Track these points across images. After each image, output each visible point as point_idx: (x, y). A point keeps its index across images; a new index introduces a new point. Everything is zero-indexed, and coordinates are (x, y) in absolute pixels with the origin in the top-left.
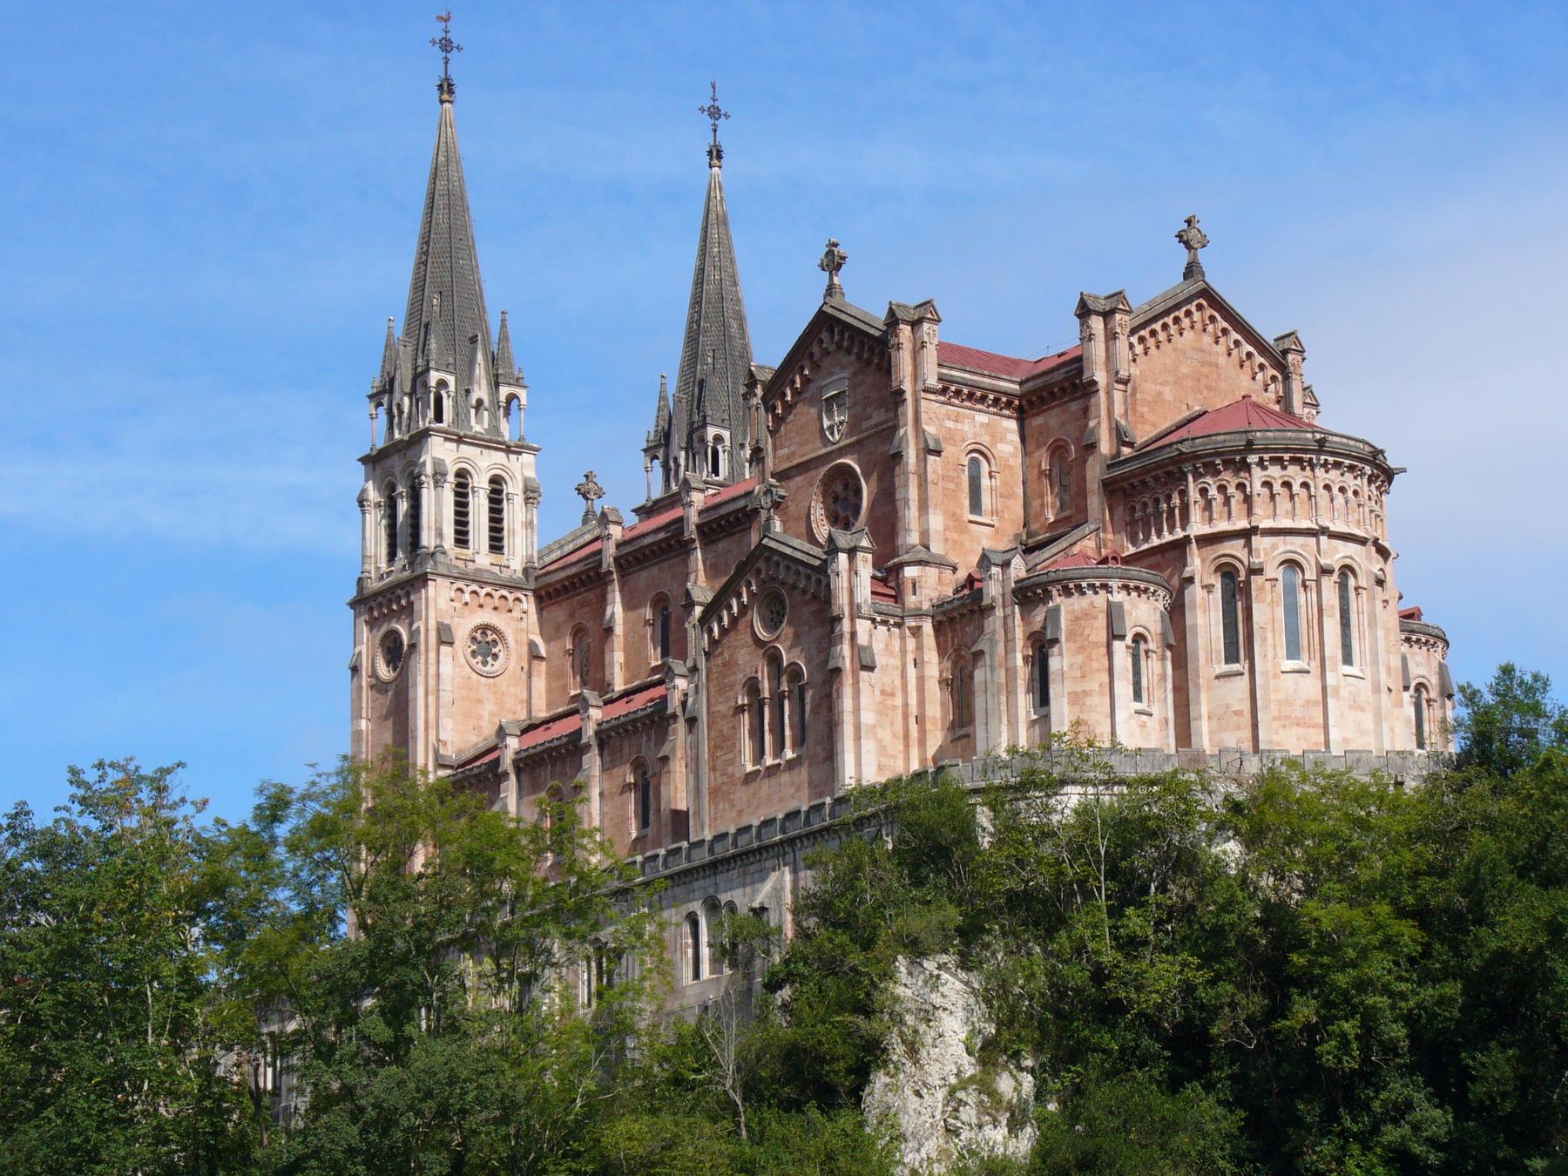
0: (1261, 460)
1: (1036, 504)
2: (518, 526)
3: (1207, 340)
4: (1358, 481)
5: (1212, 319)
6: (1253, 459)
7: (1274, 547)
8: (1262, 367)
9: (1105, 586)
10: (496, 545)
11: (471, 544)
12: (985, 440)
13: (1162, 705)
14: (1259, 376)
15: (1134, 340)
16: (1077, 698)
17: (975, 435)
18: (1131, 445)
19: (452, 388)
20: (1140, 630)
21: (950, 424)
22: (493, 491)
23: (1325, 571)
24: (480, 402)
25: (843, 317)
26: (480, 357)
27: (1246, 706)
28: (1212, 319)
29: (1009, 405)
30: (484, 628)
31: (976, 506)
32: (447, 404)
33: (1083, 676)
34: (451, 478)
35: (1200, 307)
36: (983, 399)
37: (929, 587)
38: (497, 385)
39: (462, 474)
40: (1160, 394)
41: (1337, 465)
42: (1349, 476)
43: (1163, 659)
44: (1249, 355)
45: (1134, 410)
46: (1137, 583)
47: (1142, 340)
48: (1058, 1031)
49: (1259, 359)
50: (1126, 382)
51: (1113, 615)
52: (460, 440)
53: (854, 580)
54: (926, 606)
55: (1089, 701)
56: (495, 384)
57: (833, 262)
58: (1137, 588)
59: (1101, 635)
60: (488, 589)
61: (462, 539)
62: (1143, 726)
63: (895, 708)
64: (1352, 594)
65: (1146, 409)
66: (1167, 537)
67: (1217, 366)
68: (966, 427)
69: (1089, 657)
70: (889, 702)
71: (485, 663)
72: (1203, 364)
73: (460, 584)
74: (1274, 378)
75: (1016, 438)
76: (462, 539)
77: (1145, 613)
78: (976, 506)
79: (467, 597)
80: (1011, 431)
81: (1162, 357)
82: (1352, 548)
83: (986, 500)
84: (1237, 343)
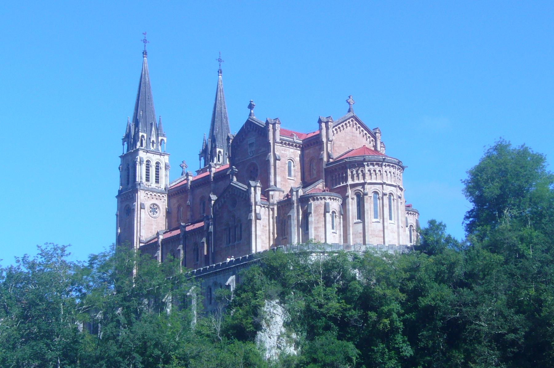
3: (354, 129)
5: (356, 124)
7: (371, 188)
8: (369, 137)
9: (324, 198)
10: (157, 181)
12: (293, 156)
13: (340, 231)
14: (368, 140)
15: (334, 129)
16: (316, 229)
18: (332, 159)
19: (145, 137)
22: (156, 166)
23: (384, 194)
24: (153, 141)
26: (153, 129)
27: (362, 231)
28: (356, 124)
29: (299, 147)
30: (154, 204)
31: (290, 174)
32: (144, 142)
34: (145, 162)
35: (352, 121)
36: (292, 145)
37: (277, 197)
38: (158, 137)
39: (148, 161)
41: (389, 165)
42: (392, 168)
43: (340, 218)
44: (366, 134)
47: (336, 130)
48: (308, 322)
49: (368, 135)
50: (331, 141)
51: (326, 206)
52: (147, 152)
53: (256, 195)
54: (275, 202)
57: (251, 107)
59: (323, 212)
60: (155, 194)
61: (148, 179)
62: (334, 236)
64: (392, 201)
66: (342, 185)
68: (287, 153)
70: (265, 229)
71: (154, 214)
73: (147, 192)
74: (372, 140)
76: (148, 179)
77: (335, 205)
78: (290, 174)
79: (149, 196)
81: (342, 134)
82: (393, 188)
83: (293, 173)
84: (362, 131)
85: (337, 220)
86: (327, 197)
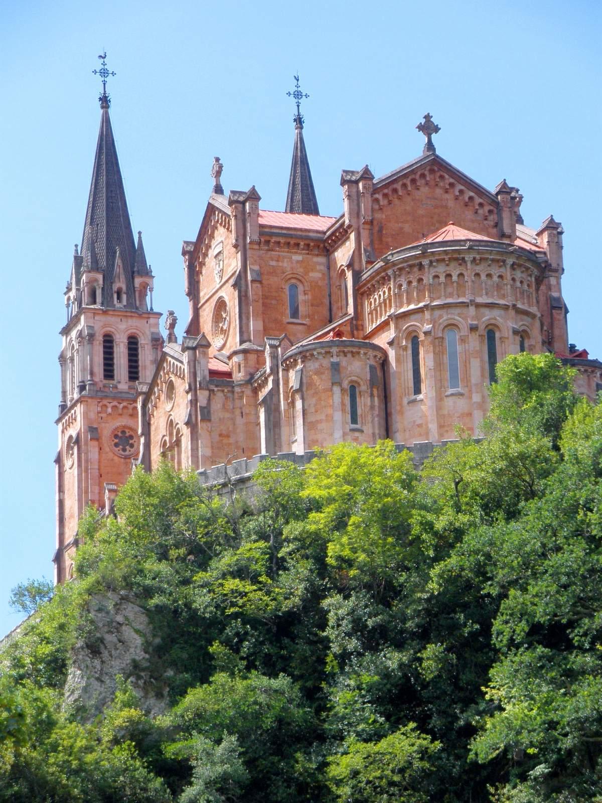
0: (431, 262)
1: (334, 308)
2: (148, 363)
3: (439, 191)
4: (502, 270)
5: (442, 177)
6: (425, 262)
7: (441, 317)
8: (481, 205)
9: (328, 353)
10: (134, 375)
11: (115, 377)
12: (300, 270)
14: (480, 211)
17: (292, 269)
20: (354, 378)
21: (273, 263)
22: (129, 343)
23: (473, 329)
25: (93, 190)
31: (295, 313)
33: (316, 411)
35: (432, 171)
36: (297, 245)
38: (133, 278)
40: (401, 229)
43: (372, 395)
45: (381, 240)
46: (350, 349)
49: (478, 200)
52: (105, 312)
55: (320, 426)
56: (131, 276)
58: (352, 352)
60: (125, 404)
63: (230, 444)
65: (390, 240)
67: (446, 207)
68: (285, 264)
69: (320, 399)
70: (225, 441)
72: (436, 207)
73: (105, 402)
74: (490, 212)
75: (323, 268)
78: (295, 313)
80: (320, 264)
82: (496, 313)
83: (302, 309)
84: (461, 191)
85: (364, 402)
86: (334, 350)
